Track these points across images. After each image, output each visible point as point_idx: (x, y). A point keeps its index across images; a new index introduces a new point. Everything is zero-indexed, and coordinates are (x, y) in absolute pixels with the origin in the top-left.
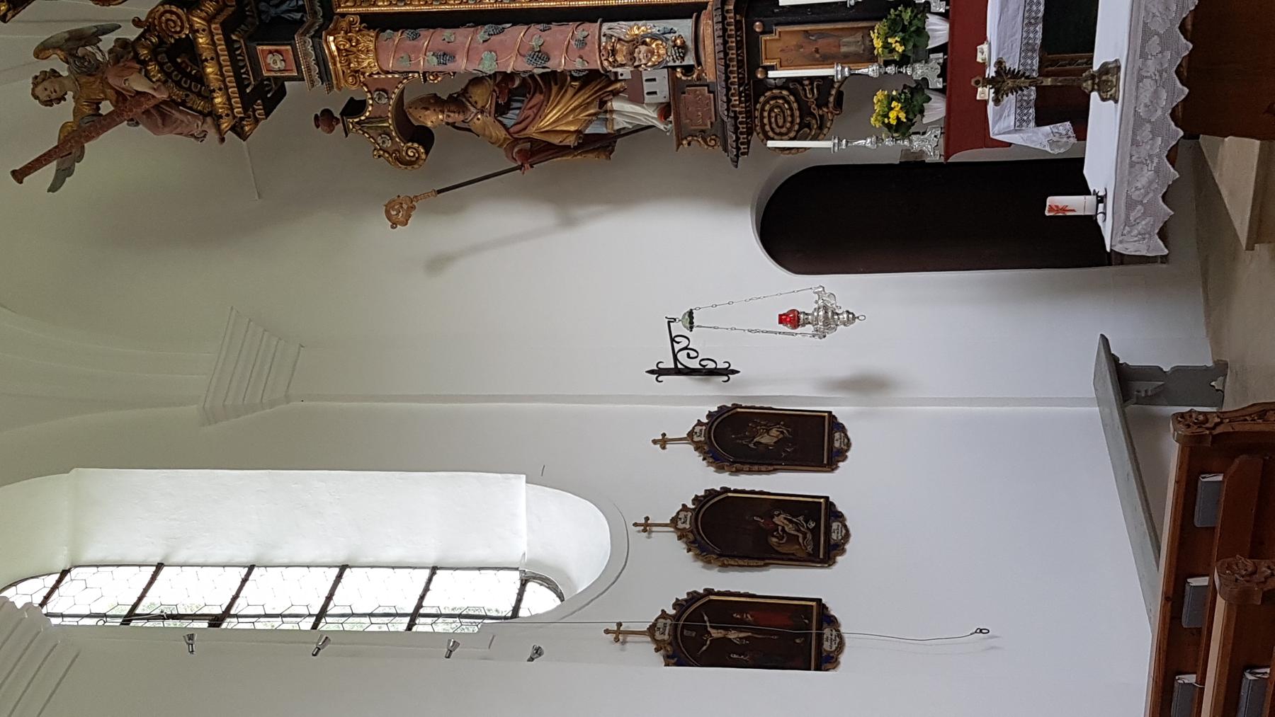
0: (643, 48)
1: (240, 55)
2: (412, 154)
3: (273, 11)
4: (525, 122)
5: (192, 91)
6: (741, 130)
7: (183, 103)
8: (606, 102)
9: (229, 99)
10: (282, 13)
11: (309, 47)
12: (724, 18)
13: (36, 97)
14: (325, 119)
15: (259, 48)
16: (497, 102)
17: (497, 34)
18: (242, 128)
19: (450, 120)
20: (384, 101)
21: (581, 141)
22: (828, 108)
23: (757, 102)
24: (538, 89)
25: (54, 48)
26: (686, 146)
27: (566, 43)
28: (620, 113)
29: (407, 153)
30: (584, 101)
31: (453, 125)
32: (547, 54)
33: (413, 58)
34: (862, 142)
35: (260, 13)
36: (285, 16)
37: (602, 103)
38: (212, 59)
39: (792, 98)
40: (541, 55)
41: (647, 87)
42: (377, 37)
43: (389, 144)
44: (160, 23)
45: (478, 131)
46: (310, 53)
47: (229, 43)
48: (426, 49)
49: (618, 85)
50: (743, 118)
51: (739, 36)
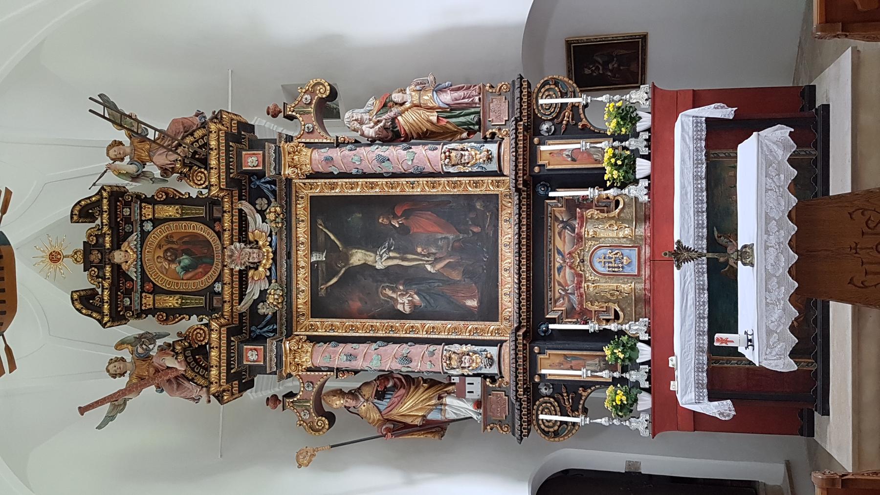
0: (467, 357)
1: (233, 349)
2: (320, 424)
4: (392, 407)
5: (200, 375)
6: (524, 419)
7: (192, 380)
8: (442, 398)
9: (220, 373)
12: (516, 339)
13: (108, 371)
14: (273, 400)
15: (245, 347)
16: (377, 389)
18: (223, 397)
19: (347, 405)
20: (310, 389)
21: (424, 422)
22: (578, 412)
23: (534, 404)
24: (403, 386)
25: (128, 344)
26: (489, 430)
27: (423, 352)
28: (450, 406)
29: (317, 424)
30: (430, 395)
31: (347, 408)
32: (411, 358)
33: (332, 356)
34: (599, 421)
35: (251, 332)
36: (264, 334)
37: (440, 398)
38: (217, 347)
39: (556, 404)
40: (407, 359)
41: (468, 388)
42: (314, 346)
43: (307, 417)
44: (193, 335)
45: (363, 414)
47: (229, 341)
49: (450, 388)
50: (525, 425)
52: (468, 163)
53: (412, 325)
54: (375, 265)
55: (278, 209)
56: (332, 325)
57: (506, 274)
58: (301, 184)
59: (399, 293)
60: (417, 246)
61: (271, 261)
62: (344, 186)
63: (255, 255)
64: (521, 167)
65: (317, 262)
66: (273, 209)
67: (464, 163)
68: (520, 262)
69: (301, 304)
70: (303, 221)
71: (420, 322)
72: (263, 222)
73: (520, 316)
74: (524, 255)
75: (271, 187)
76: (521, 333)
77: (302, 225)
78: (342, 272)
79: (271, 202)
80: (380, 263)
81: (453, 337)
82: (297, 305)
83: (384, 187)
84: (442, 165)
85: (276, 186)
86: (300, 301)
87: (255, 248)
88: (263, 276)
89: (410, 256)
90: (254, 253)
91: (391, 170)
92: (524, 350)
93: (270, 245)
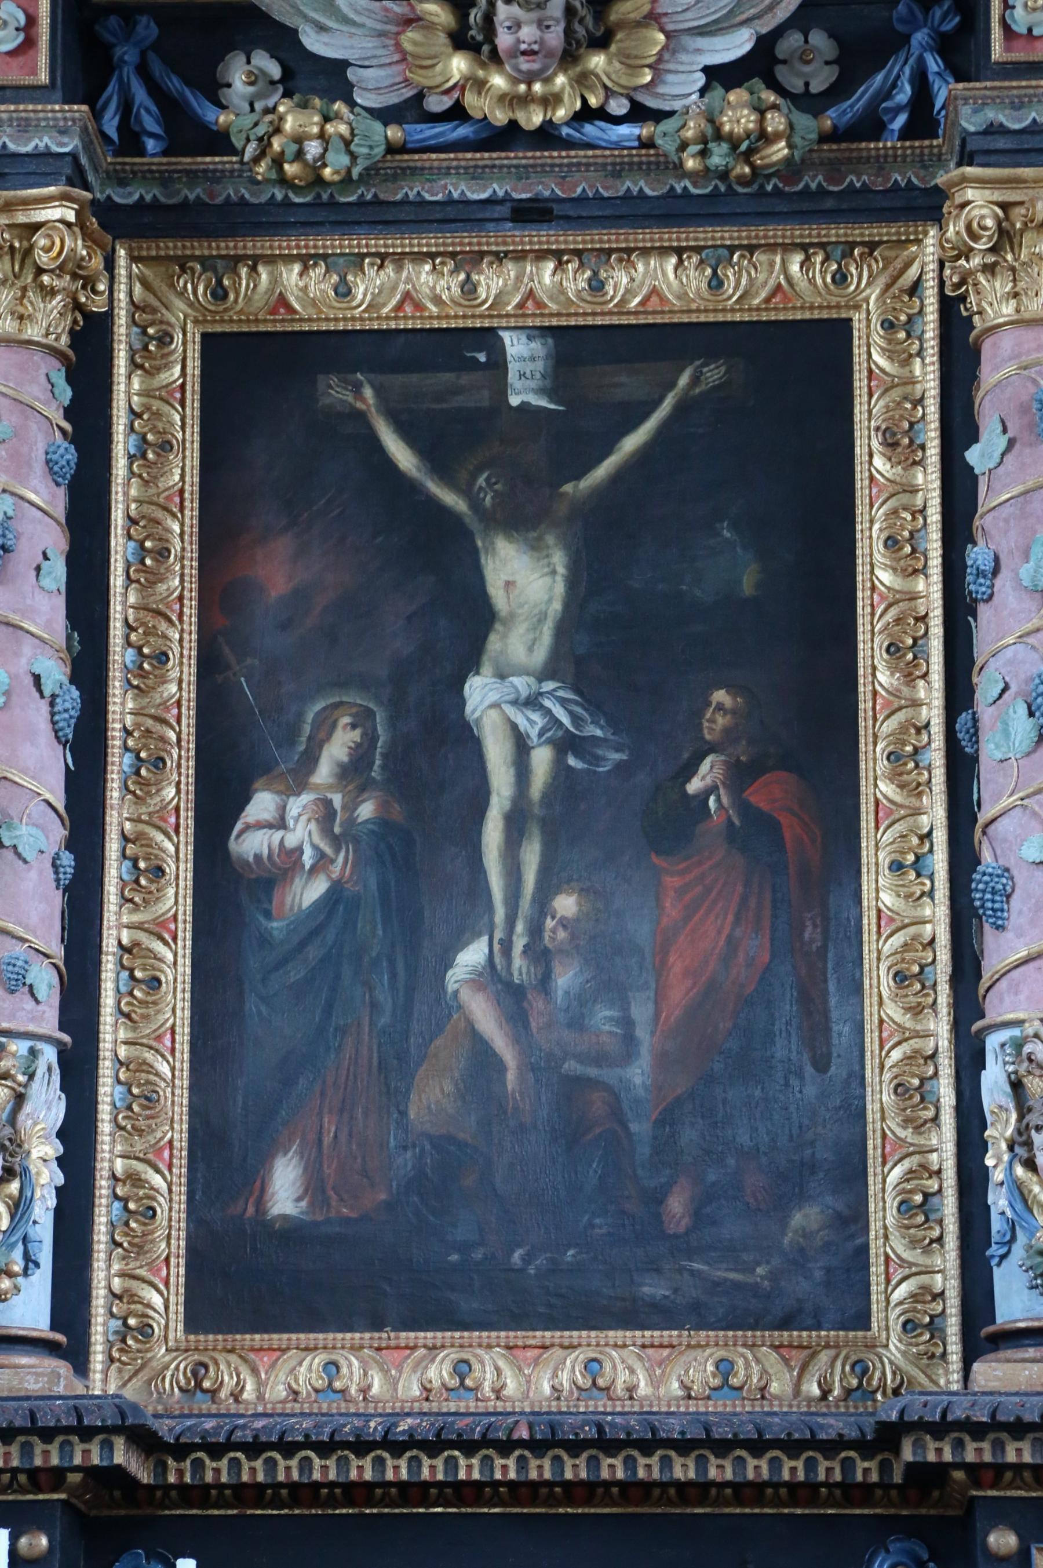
3: (127, 54)
10: (120, 79)
11: (46, 139)
12: (86, 1433)
17: (54, 723)
27: (20, 932)
35: (129, 15)
36: (112, 87)
42: (55, 352)
46: (30, 140)
48: (22, 498)
51: (14, 1478)
52: (1030, 1164)
53: (170, 868)
54: (487, 668)
55: (779, 151)
56: (165, 446)
57: (439, 1372)
58: (913, 272)
59: (337, 799)
60: (583, 892)
61: (500, 117)
62: (904, 498)
63: (528, 33)
64: (1011, 1457)
65: (498, 363)
66: (775, 122)
67: (1029, 1144)
68: (505, 1447)
69: (275, 281)
70: (716, 283)
71: (186, 909)
72: (707, 70)
73: (216, 1451)
74: (541, 1469)
75: (897, 110)
76: (121, 1455)
77: (696, 280)
78: (450, 498)
79: (816, 113)
80: (493, 697)
81: (108, 1092)
82: (271, 260)
83: (901, 716)
84: (1019, 1023)
85: (905, 134)
86: (291, 275)
87: (568, 32)
88: (421, 79)
89: (531, 856)
90: (542, 25)
91: (990, 751)
92: (33, 1473)
93: (586, 114)
